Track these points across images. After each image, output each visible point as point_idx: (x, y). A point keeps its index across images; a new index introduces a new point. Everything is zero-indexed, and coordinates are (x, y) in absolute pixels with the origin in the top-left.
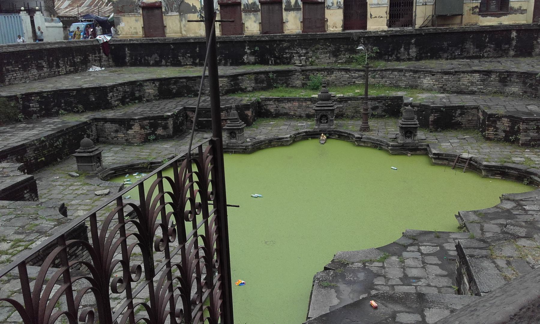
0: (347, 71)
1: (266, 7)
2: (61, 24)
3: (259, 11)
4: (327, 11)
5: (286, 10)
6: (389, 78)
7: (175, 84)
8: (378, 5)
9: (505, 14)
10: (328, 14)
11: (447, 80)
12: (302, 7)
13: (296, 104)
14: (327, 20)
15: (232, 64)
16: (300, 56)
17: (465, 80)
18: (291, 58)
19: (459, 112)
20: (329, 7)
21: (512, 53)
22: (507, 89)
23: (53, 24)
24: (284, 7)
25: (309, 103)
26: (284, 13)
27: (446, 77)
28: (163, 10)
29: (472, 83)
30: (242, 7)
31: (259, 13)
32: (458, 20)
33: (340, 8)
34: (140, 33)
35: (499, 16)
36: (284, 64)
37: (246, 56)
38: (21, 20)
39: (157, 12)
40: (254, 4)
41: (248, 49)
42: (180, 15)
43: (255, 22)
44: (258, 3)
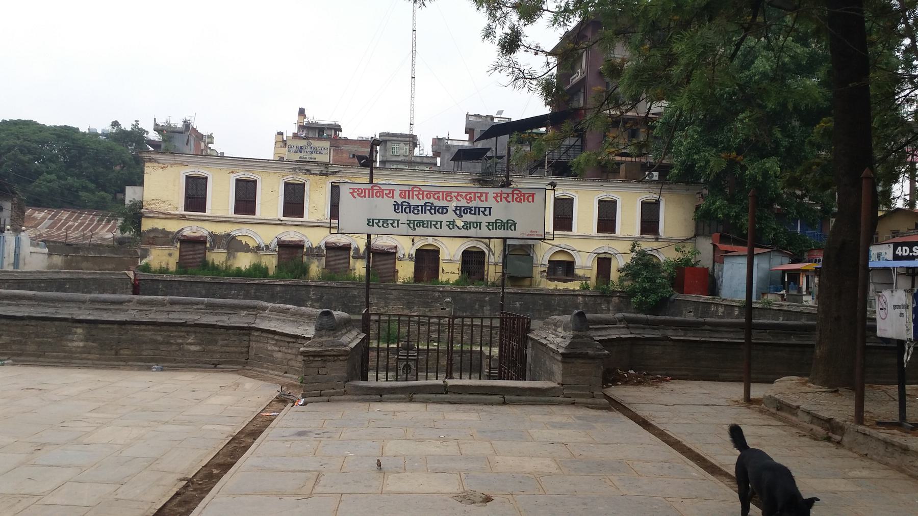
1: (332, 253)
2: (46, 250)
4: (397, 261)
8: (451, 261)
9: (571, 280)
10: (399, 266)
20: (400, 259)
23: (38, 249)
24: (352, 253)
26: (352, 260)
28: (208, 245)
31: (324, 258)
32: (527, 282)
33: (411, 260)
34: (173, 267)
35: (565, 281)
38: (4, 241)
39: (200, 247)
40: (319, 248)
42: (228, 253)
44: (323, 247)
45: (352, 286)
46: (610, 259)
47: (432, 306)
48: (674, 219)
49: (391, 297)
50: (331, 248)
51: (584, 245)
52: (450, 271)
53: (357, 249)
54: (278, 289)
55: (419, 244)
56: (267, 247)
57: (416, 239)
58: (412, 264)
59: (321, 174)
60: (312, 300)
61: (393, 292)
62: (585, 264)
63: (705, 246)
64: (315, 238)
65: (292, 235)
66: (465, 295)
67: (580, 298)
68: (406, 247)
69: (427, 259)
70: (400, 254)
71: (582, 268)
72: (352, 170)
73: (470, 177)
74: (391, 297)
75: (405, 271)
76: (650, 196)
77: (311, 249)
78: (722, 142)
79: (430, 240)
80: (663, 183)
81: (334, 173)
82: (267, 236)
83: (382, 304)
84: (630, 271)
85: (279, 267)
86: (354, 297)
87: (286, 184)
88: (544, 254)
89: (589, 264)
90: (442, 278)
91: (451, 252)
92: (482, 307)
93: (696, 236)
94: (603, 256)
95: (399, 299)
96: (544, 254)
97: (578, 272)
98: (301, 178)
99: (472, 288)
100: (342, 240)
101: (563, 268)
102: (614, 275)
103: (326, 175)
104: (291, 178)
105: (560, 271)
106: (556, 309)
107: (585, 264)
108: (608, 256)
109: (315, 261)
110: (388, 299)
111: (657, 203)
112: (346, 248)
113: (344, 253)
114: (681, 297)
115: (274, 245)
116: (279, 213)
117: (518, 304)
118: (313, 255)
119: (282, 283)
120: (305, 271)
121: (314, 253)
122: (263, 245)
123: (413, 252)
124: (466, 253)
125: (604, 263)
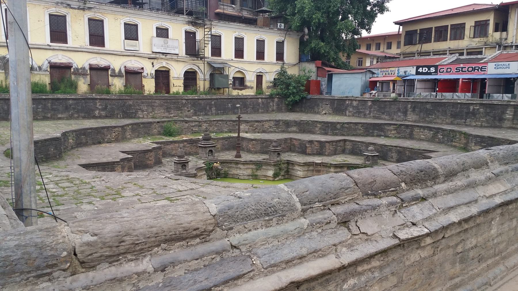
0: (187, 122)
1: (94, 72)
3: (87, 75)
5: (111, 76)
6: (216, 126)
7: (84, 134)
8: (178, 78)
9: (244, 89)
10: (145, 82)
11: (257, 126)
12: (124, 74)
13: (177, 145)
14: (144, 86)
15: (84, 118)
16: (143, 111)
17: (267, 125)
18: (136, 112)
19: (283, 142)
20: (145, 77)
21: (260, 111)
22: (289, 130)
24: (110, 73)
25: (185, 143)
26: (110, 78)
27: (256, 124)
29: (270, 127)
30: (72, 70)
31: (89, 77)
33: (152, 78)
35: (241, 90)
36: (132, 118)
37: (98, 112)
40: (83, 69)
41: (100, 105)
43: (84, 83)
45: (127, 98)
46: (262, 76)
47: (182, 110)
48: (291, 52)
49: (156, 104)
50: (92, 68)
51: (249, 68)
52: (177, 85)
53: (114, 70)
54: (71, 102)
55: (157, 67)
56: (40, 68)
57: (155, 61)
58: (153, 80)
59: (79, 9)
60: (99, 109)
61: (157, 101)
62: (251, 79)
63: (311, 68)
64: (81, 61)
65: (60, 58)
66: (200, 101)
67: (260, 100)
68: (149, 69)
69: (162, 77)
70: (144, 74)
71: (250, 81)
72: (105, 7)
73: (187, 20)
74: (156, 104)
75: (149, 86)
76: (280, 39)
77: (77, 69)
78: (323, 9)
79: (164, 64)
80: (287, 31)
81: (90, 8)
82: (40, 59)
83: (150, 110)
84: (275, 83)
85: (52, 83)
86: (130, 105)
87: (50, 15)
88: (231, 73)
89: (253, 79)
90: (173, 90)
91: (177, 72)
92: (210, 108)
93: (299, 62)
94: (259, 74)
95: (161, 106)
96: (231, 73)
97: (248, 84)
98: (62, 11)
99: (190, 97)
100: (101, 61)
101: (240, 82)
102: (264, 85)
103: (83, 9)
104: (54, 10)
105: (237, 82)
106: (249, 107)
107: (251, 79)
108: (261, 74)
109: (81, 79)
110: (154, 106)
111: (283, 42)
112: (106, 69)
113: (104, 73)
114: (309, 96)
115: (46, 66)
116: (47, 39)
117: (229, 105)
118: (80, 74)
119: (73, 97)
120: (74, 86)
121: (80, 72)
122: (35, 66)
123: (153, 72)
124: (187, 73)
125: (259, 78)
